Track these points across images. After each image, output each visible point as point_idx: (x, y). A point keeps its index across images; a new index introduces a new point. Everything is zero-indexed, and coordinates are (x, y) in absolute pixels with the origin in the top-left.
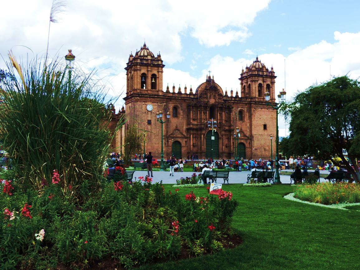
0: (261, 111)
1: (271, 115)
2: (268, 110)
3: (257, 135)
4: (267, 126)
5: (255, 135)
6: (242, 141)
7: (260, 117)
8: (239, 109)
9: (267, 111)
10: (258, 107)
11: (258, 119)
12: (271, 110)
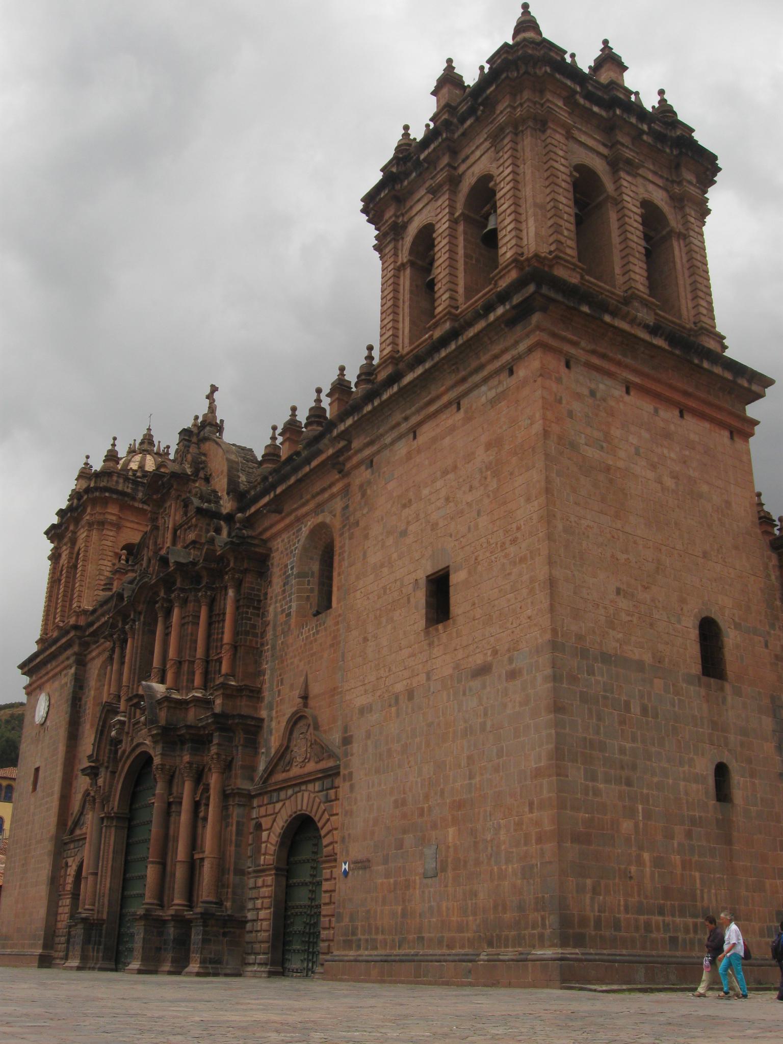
0: (409, 456)
1: (488, 446)
2: (461, 414)
3: (374, 717)
4: (454, 579)
5: (362, 711)
6: (305, 800)
7: (406, 511)
8: (305, 531)
9: (452, 429)
10: (388, 439)
11: (390, 541)
12: (483, 399)
